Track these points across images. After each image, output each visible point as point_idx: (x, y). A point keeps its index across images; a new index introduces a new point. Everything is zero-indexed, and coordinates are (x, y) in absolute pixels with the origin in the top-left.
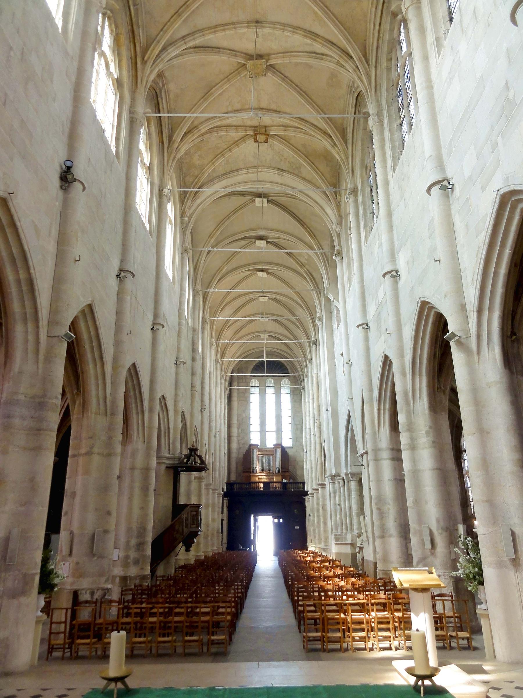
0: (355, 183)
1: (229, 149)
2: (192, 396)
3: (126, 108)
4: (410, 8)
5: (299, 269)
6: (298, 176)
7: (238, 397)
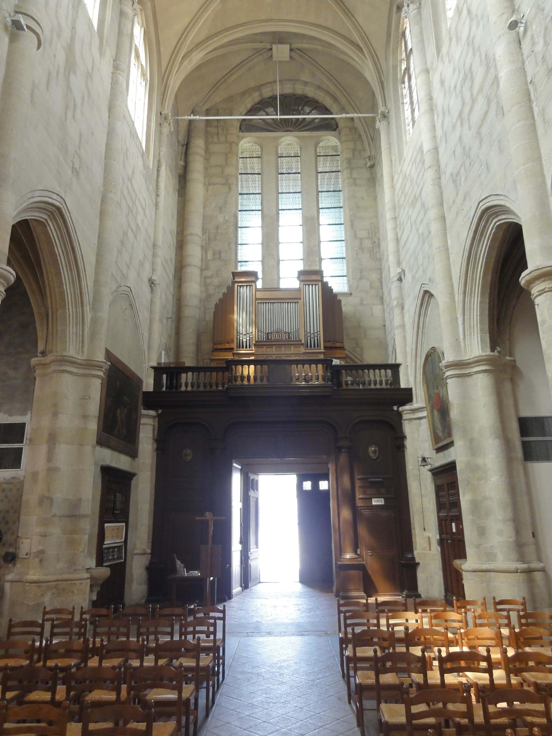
7: (207, 175)
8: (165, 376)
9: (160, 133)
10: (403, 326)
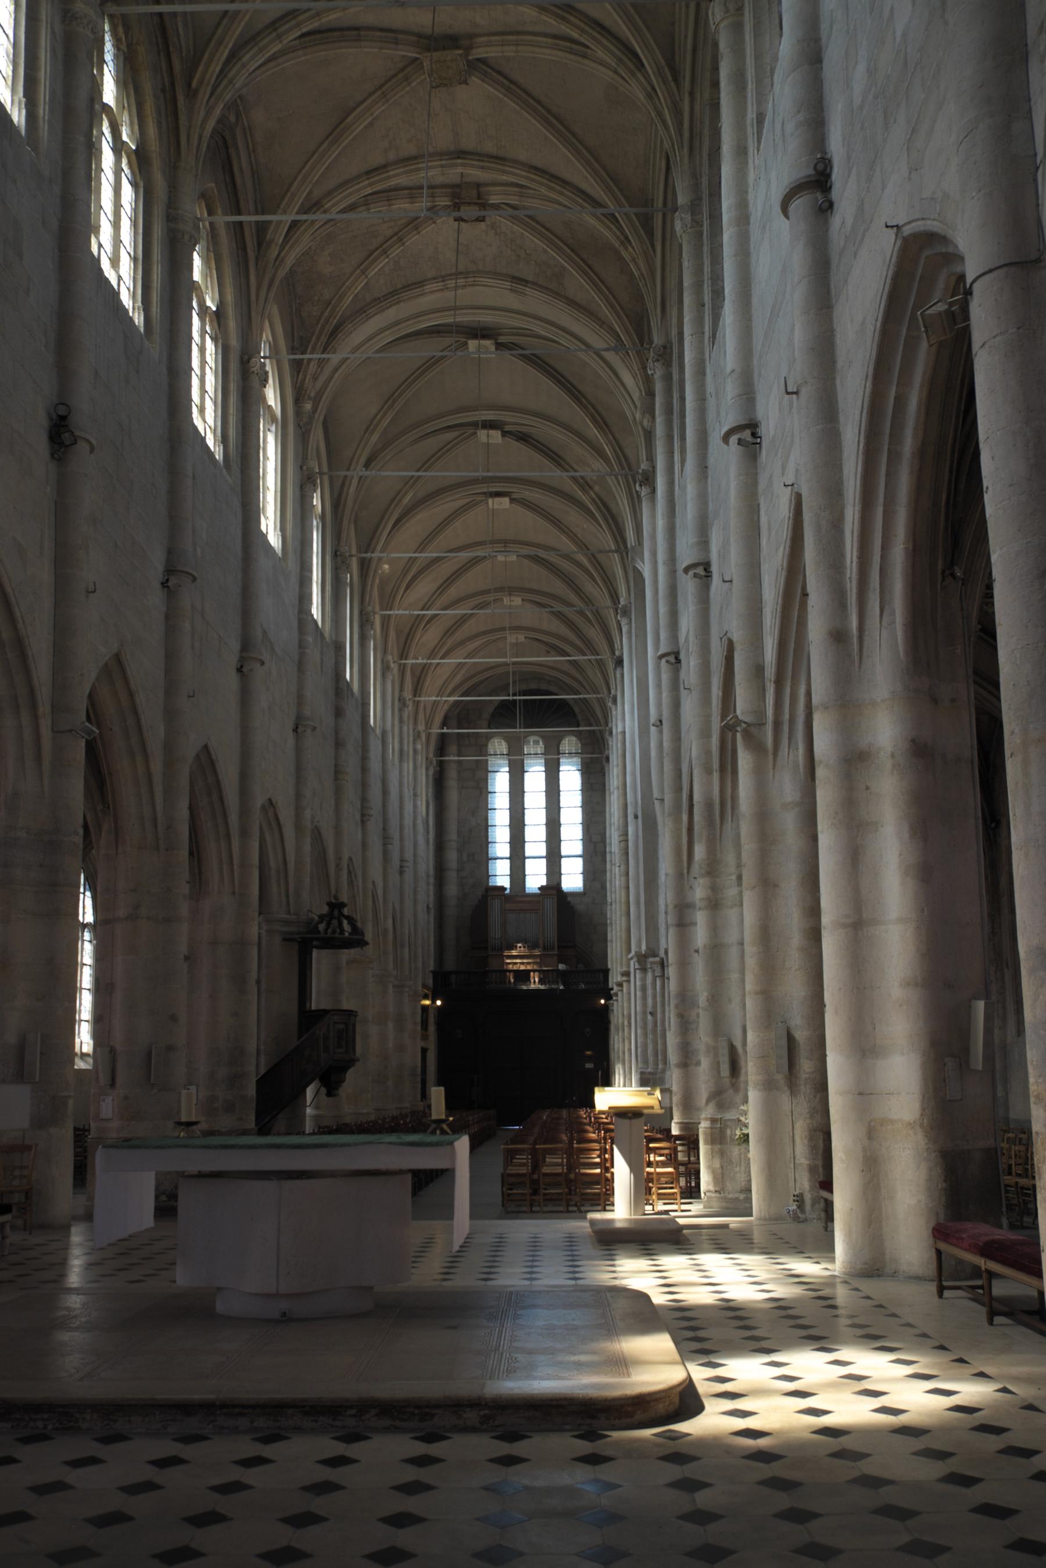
0: (667, 334)
1: (398, 236)
2: (338, 791)
3: (159, 211)
4: (722, 25)
5: (580, 494)
6: (557, 294)
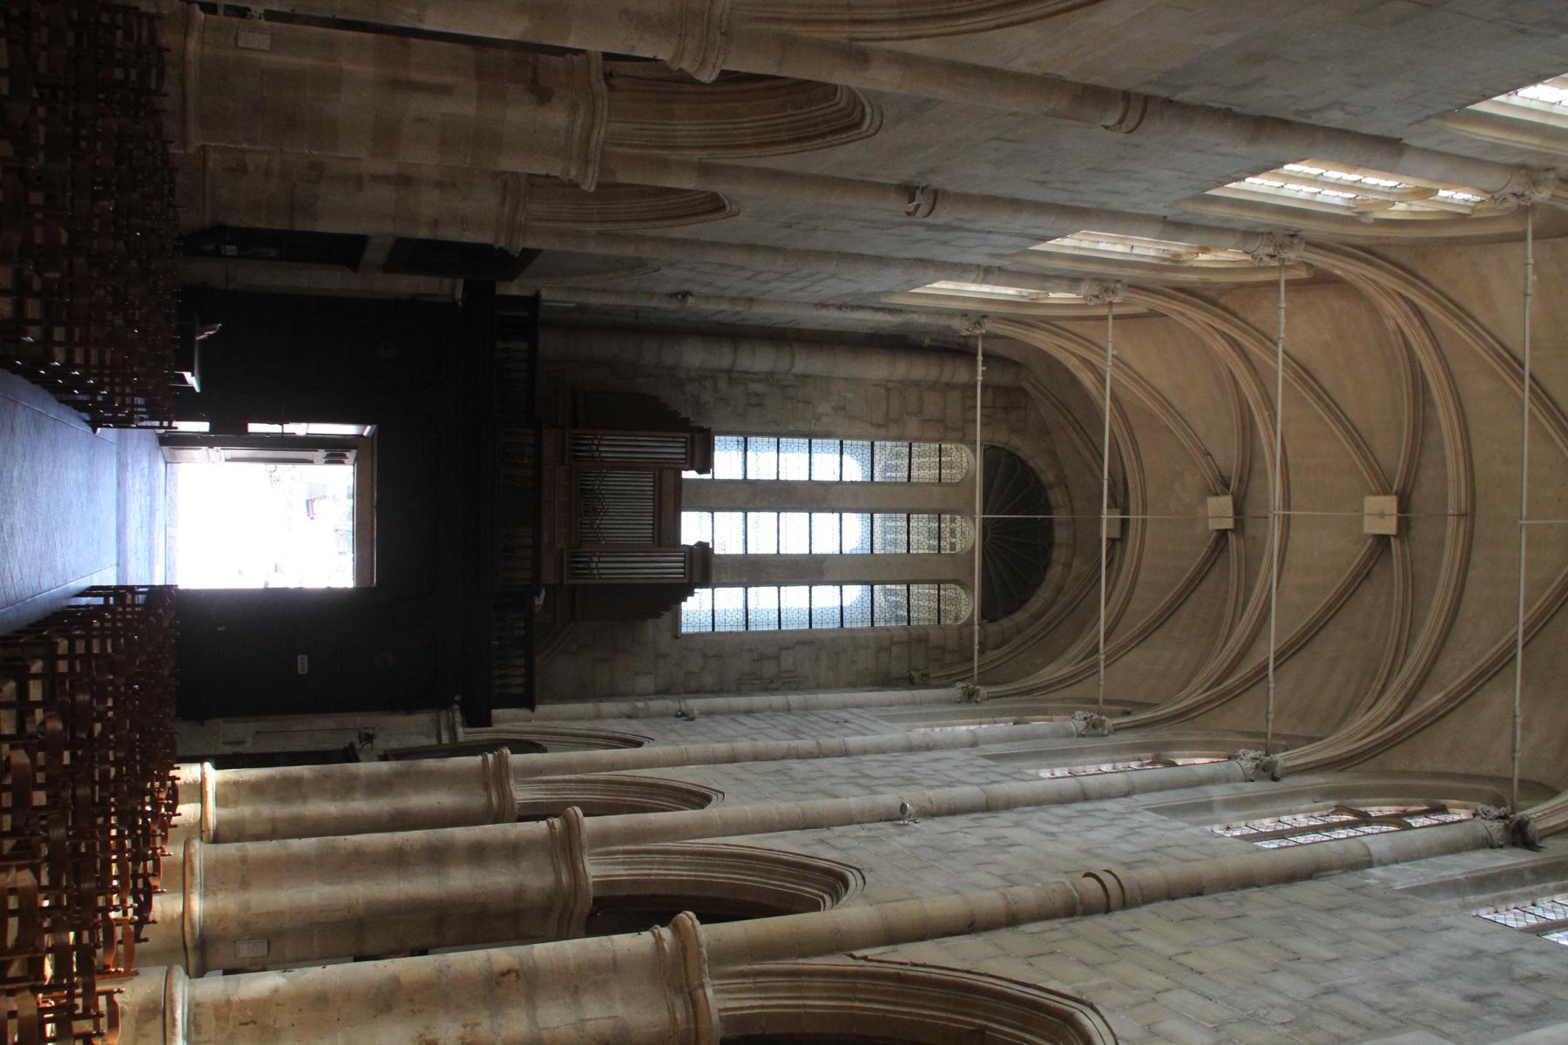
7: (908, 384)
8: (526, 314)
9: (952, 314)
10: (598, 716)
